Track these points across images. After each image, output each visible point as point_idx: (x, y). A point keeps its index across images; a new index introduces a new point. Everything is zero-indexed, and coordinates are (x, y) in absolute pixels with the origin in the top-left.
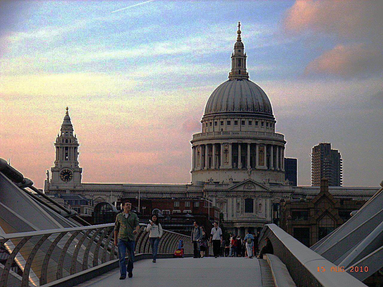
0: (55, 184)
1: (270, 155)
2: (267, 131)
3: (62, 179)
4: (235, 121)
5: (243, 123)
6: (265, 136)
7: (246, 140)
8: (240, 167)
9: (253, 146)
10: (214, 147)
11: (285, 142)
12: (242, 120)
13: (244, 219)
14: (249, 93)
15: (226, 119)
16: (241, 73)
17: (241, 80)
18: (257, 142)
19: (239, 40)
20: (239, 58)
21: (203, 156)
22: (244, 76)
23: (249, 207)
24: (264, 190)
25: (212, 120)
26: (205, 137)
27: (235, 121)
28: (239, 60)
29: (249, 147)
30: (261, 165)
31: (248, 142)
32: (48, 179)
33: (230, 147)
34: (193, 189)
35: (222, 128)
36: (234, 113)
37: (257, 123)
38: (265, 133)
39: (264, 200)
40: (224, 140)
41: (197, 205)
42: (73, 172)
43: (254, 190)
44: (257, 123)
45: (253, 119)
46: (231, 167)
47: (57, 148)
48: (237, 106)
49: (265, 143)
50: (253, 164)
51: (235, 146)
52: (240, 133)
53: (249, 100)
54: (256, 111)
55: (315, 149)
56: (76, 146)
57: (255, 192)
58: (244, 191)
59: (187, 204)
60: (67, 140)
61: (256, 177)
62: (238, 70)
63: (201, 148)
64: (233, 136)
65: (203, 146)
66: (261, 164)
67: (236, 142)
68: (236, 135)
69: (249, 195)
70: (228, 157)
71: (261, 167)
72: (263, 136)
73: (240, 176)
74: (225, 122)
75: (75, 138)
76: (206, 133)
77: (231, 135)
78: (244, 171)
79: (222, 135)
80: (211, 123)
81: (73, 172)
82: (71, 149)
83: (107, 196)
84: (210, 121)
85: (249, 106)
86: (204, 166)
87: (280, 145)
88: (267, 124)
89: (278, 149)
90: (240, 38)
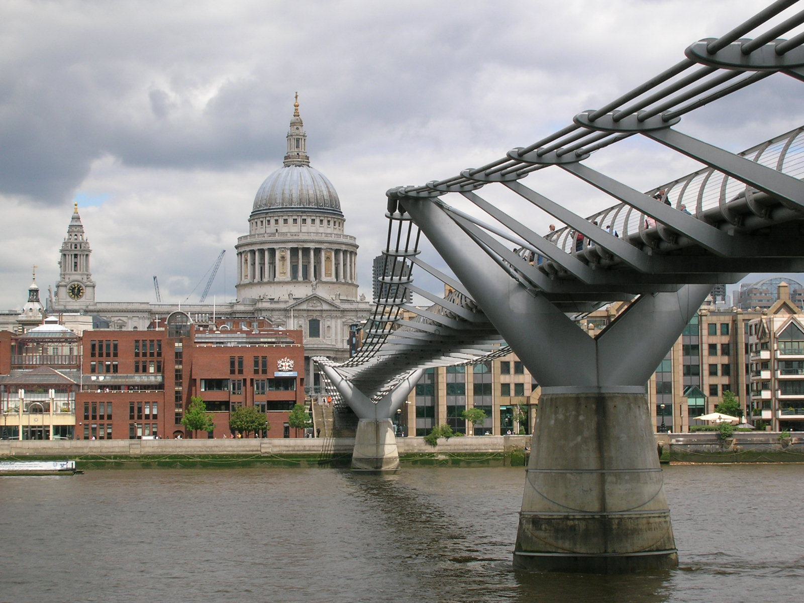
0: (62, 303)
1: (339, 264)
2: (335, 232)
3: (71, 296)
4: (294, 220)
5: (304, 221)
6: (333, 239)
7: (308, 244)
8: (300, 278)
9: (318, 251)
10: (266, 253)
11: (357, 247)
12: (303, 217)
13: (308, 346)
14: (310, 182)
15: (282, 216)
16: (301, 157)
17: (300, 166)
18: (322, 246)
19: (296, 115)
20: (297, 138)
21: (252, 265)
22: (303, 161)
23: (314, 329)
24: (333, 308)
25: (263, 218)
26: (254, 240)
27: (294, 220)
28: (298, 140)
29: (312, 253)
30: (328, 276)
31: (311, 247)
32: (50, 296)
33: (289, 252)
35: (276, 228)
36: (293, 208)
37: (321, 221)
38: (333, 235)
39: (333, 321)
40: (280, 244)
42: (84, 287)
43: (321, 308)
44: (321, 221)
45: (317, 216)
46: (289, 279)
47: (65, 255)
49: (333, 248)
51: (294, 251)
52: (300, 234)
53: (311, 192)
54: (320, 206)
55: (377, 261)
56: (86, 253)
57: (322, 310)
58: (308, 310)
60: (76, 245)
61: (322, 292)
62: (296, 153)
63: (249, 255)
64: (291, 238)
66: (328, 274)
67: (296, 246)
68: (296, 238)
69: (315, 315)
70: (284, 267)
72: (330, 239)
73: (302, 291)
74: (281, 221)
75: (87, 243)
76: (256, 235)
77: (289, 238)
78: (306, 284)
79: (277, 238)
80: (262, 222)
81: (84, 287)
82: (82, 257)
83: (129, 318)
84: (261, 219)
85: (312, 200)
86: (254, 278)
87: (352, 250)
88: (335, 222)
89: (348, 255)
90: (298, 113)
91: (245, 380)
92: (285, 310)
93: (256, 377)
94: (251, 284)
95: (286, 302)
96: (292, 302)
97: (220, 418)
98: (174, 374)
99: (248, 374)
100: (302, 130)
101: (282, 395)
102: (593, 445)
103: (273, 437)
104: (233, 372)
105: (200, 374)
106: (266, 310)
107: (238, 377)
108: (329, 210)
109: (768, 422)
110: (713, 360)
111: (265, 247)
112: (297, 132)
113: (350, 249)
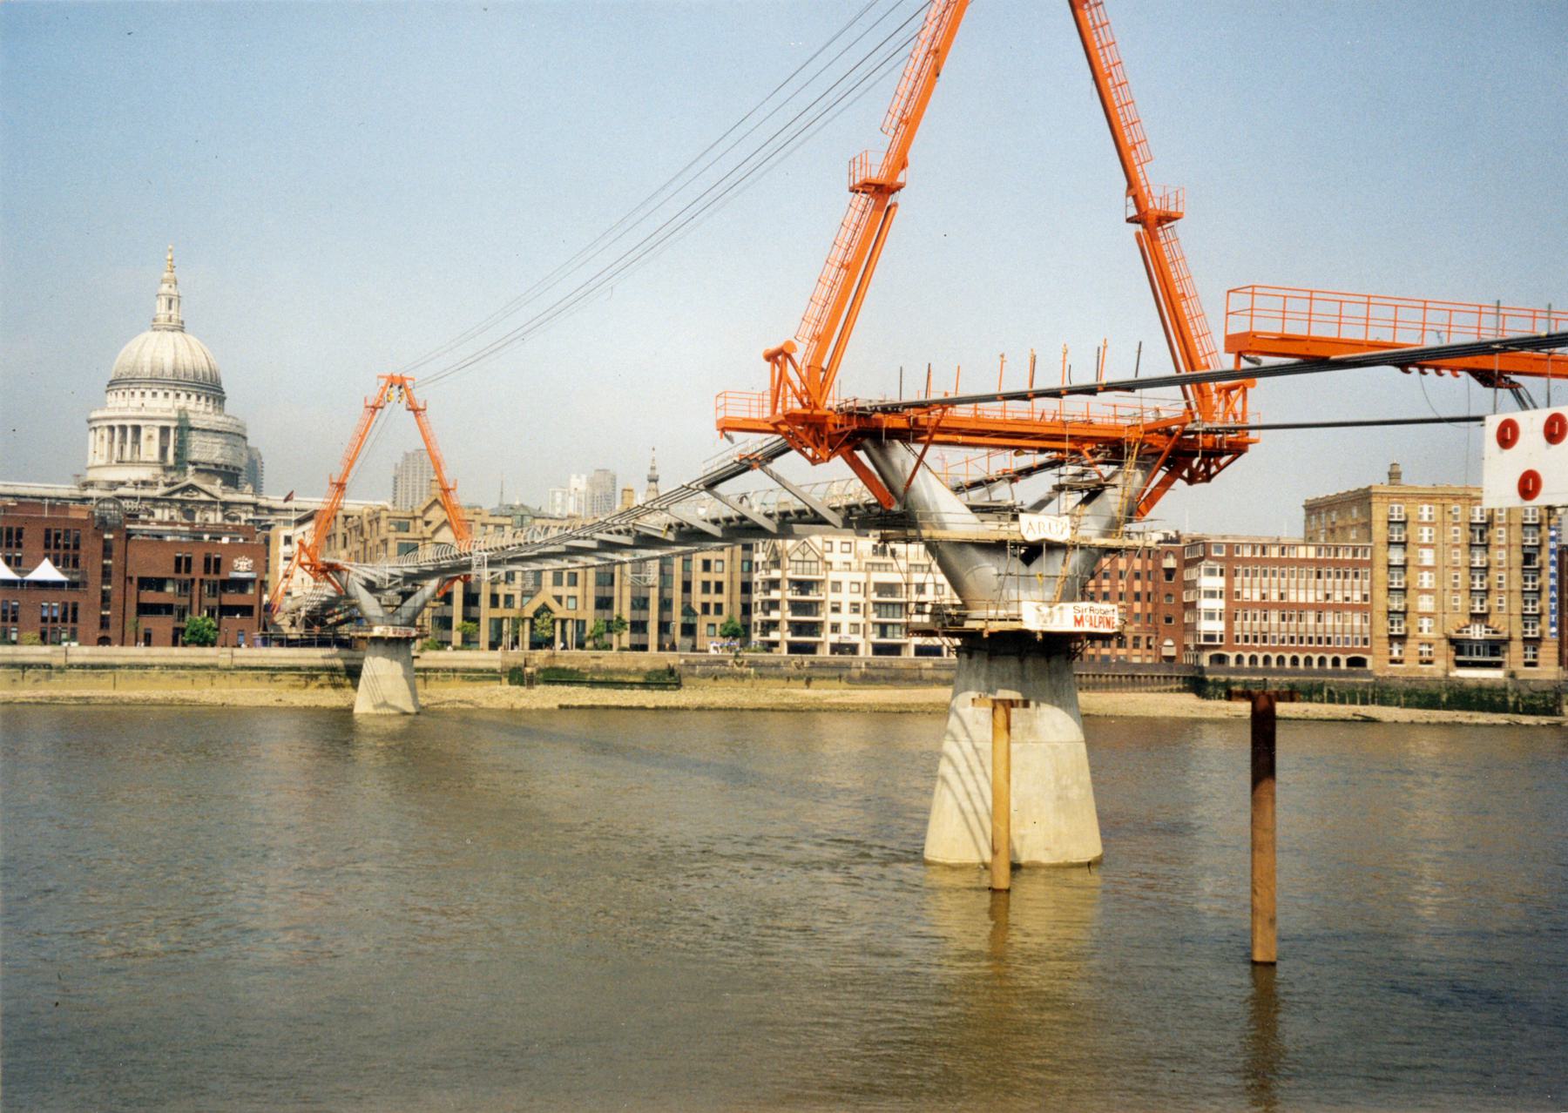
48: (168, 369)
51: (164, 431)
63: (106, 433)
65: (112, 428)
74: (149, 393)
77: (158, 414)
79: (143, 413)
91: (193, 581)
92: (155, 500)
93: (207, 577)
97: (162, 625)
98: (100, 571)
99: (197, 572)
101: (231, 598)
103: (158, 645)
104: (178, 570)
105: (136, 572)
107: (184, 576)
109: (775, 644)
110: (706, 576)
111: (128, 423)
112: (172, 291)
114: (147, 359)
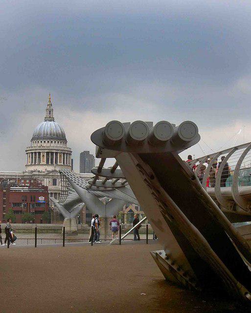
6: (62, 149)
9: (56, 153)
23: (55, 183)
34: (27, 174)
41: (32, 181)
50: (56, 162)
51: (48, 153)
55: (81, 154)
59: (28, 181)
65: (32, 153)
66: (60, 162)
69: (55, 177)
71: (60, 164)
73: (50, 168)
74: (43, 142)
79: (41, 148)
94: (31, 165)
95: (44, 172)
96: (47, 172)
100: (51, 108)
102: (104, 229)
106: (36, 175)
108: (61, 138)
113: (69, 153)
114: (43, 131)
